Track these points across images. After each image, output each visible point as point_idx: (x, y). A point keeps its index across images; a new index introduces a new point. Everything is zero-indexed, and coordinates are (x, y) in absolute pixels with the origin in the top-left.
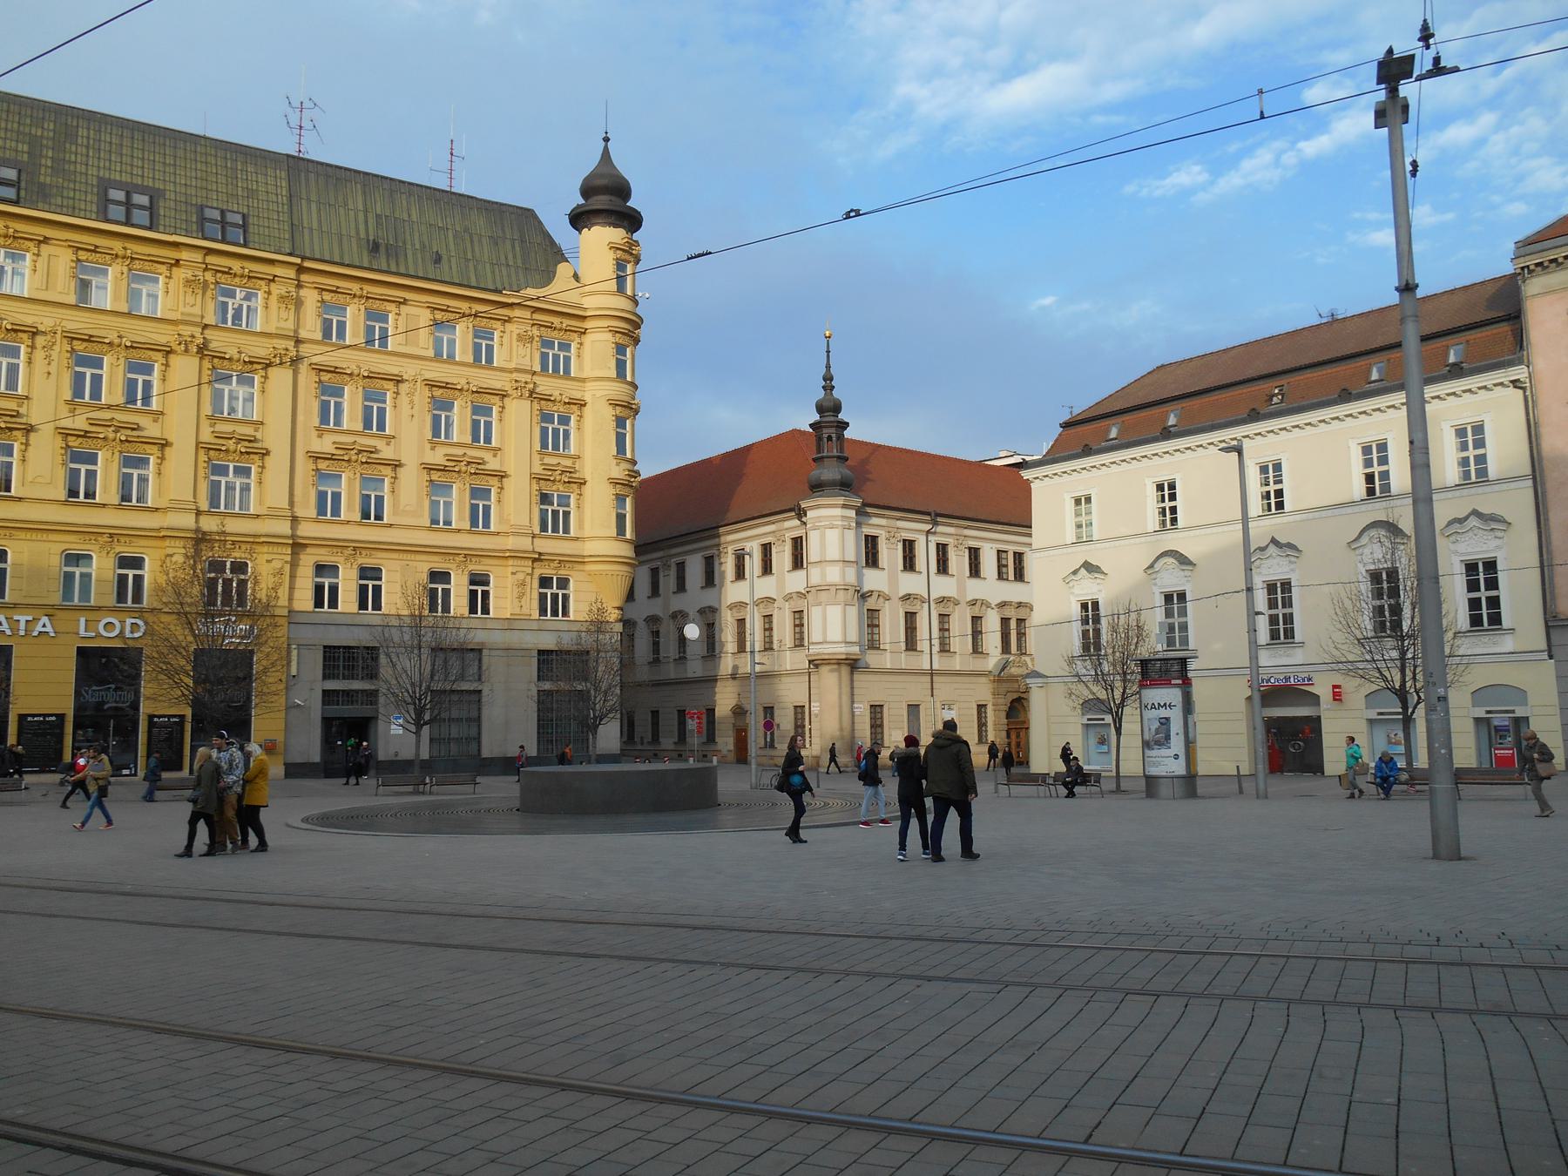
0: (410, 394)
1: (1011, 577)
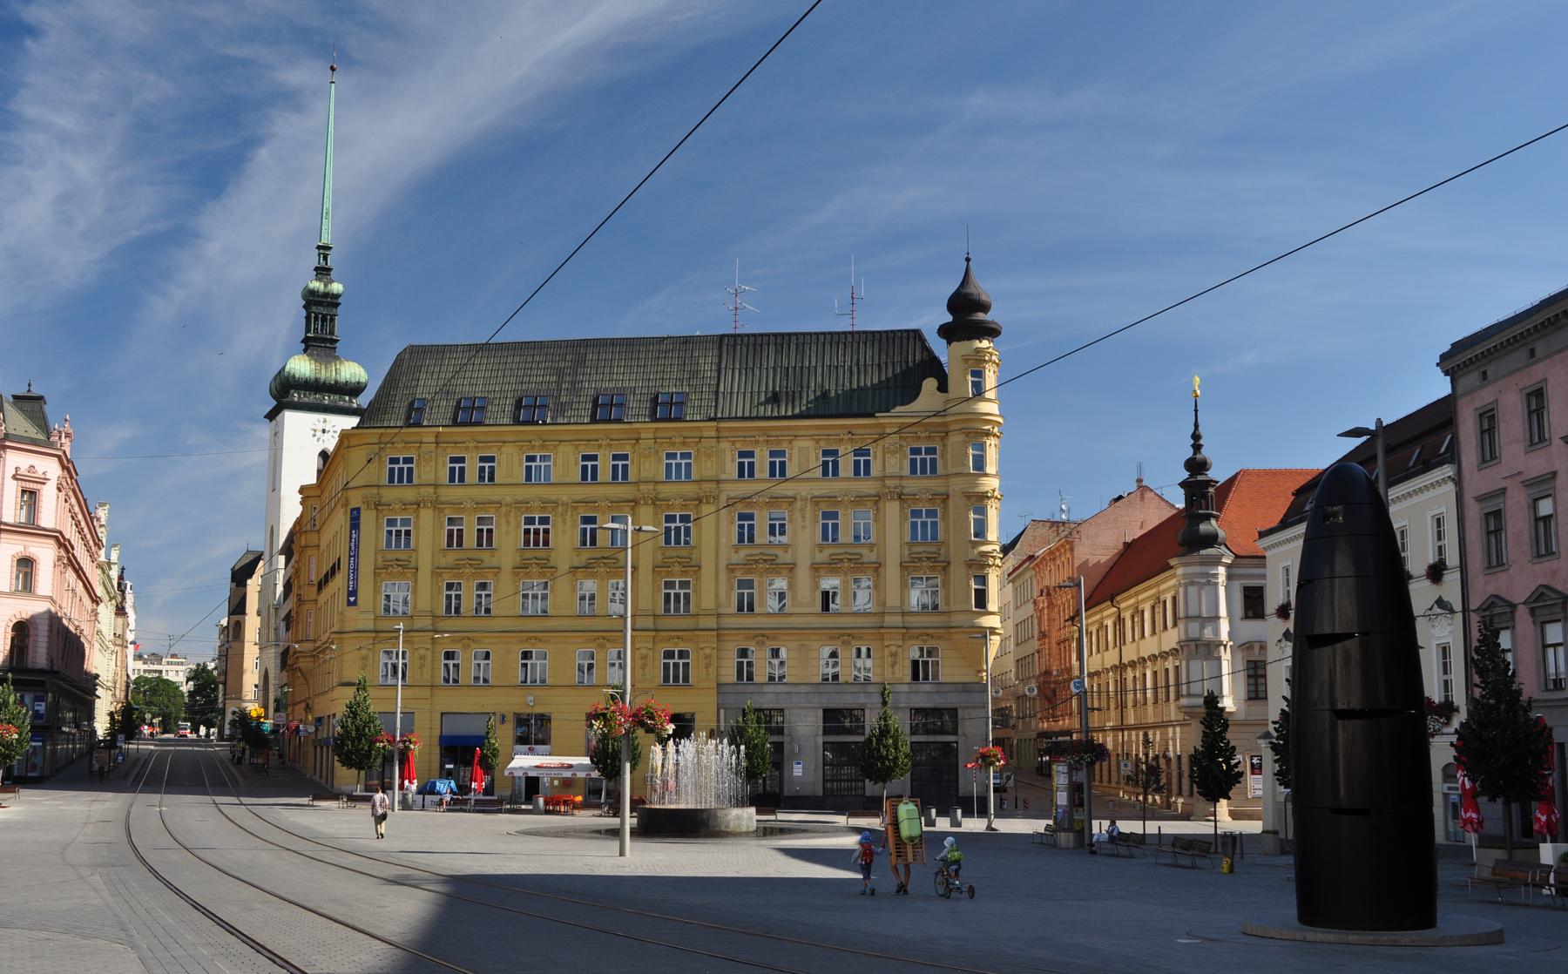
0: (802, 510)
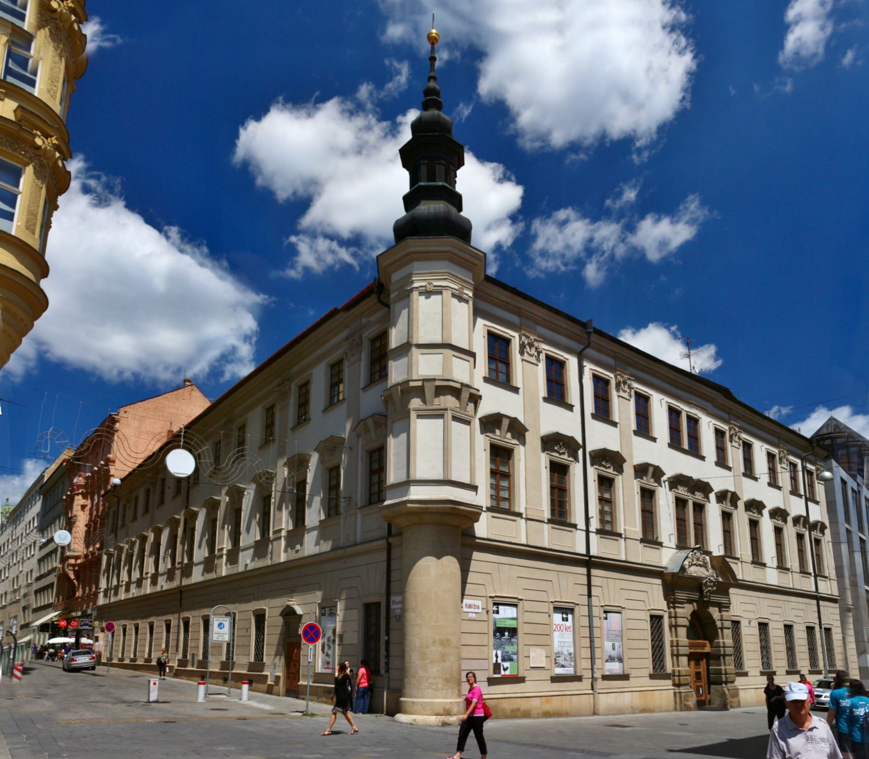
1: (686, 446)
